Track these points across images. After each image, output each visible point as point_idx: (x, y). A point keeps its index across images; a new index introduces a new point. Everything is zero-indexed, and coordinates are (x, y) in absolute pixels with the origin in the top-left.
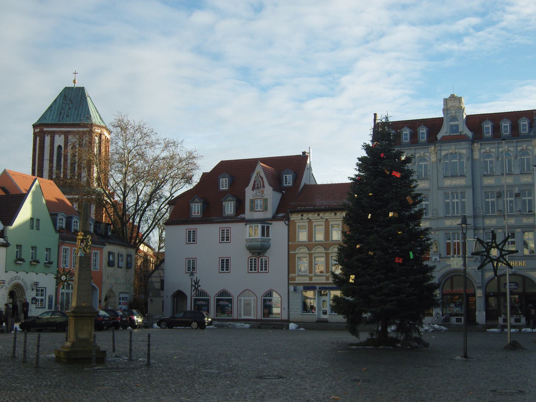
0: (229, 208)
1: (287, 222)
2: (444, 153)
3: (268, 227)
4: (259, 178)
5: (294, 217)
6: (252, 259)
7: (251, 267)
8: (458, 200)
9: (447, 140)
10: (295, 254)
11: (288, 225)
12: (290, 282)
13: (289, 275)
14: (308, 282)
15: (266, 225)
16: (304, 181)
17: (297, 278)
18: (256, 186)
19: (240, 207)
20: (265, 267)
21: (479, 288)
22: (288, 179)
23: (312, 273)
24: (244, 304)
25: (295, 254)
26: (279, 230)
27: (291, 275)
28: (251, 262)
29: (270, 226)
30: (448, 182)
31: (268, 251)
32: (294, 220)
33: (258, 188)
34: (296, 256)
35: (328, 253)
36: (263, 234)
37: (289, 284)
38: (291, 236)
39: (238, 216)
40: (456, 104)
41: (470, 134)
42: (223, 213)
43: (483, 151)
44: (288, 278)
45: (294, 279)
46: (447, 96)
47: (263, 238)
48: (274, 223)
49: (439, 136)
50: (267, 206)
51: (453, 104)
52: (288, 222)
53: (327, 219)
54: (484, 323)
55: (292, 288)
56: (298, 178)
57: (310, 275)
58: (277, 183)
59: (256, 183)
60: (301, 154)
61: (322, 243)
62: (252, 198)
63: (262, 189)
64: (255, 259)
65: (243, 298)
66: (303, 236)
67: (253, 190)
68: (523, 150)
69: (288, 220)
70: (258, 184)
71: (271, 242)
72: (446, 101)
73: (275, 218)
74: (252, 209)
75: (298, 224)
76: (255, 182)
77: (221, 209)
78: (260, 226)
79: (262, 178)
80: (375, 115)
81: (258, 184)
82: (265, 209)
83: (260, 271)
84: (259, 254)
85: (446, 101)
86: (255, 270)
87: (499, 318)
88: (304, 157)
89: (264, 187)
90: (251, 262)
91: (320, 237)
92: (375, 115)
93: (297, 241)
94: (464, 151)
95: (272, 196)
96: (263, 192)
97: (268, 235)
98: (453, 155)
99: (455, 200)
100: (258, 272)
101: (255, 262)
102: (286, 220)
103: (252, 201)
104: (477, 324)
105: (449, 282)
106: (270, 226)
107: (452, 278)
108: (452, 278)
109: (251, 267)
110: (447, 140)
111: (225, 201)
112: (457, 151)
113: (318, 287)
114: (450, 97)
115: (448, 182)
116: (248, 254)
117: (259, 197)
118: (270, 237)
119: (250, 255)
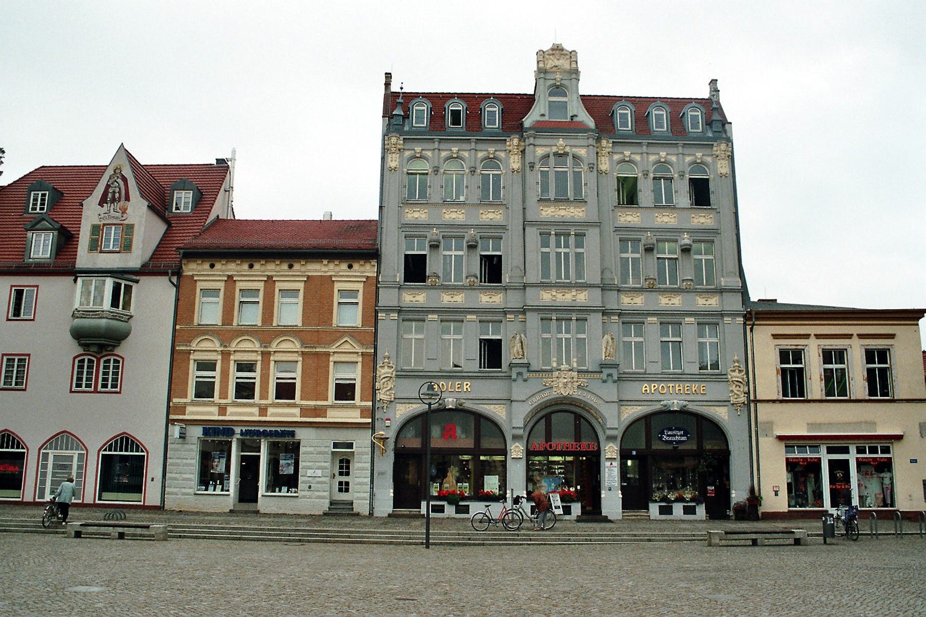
0: (42, 246)
1: (174, 279)
2: (540, 151)
3: (128, 289)
4: (119, 180)
5: (191, 269)
6: (83, 361)
7: (79, 379)
8: (567, 250)
9: (542, 128)
10: (189, 352)
11: (177, 287)
12: (172, 417)
13: (169, 400)
14: (216, 418)
15: (123, 283)
16: (218, 211)
17: (189, 409)
18: (110, 195)
19: (66, 240)
20: (113, 382)
21: (516, 438)
22: (184, 200)
23: (226, 398)
24: (55, 466)
25: (189, 352)
26: (154, 299)
27: (175, 400)
28: (81, 367)
29: (135, 286)
30: (549, 213)
31: (124, 344)
32: (192, 276)
33: (113, 200)
34: (191, 357)
35: (269, 353)
36: (115, 303)
37: (169, 422)
38: (183, 310)
39: (63, 266)
40: (564, 64)
41: (591, 123)
42: (26, 257)
43: (616, 157)
44: (168, 407)
45: (182, 409)
46: (546, 47)
47: (114, 309)
48: (143, 279)
49: (528, 121)
50: (131, 241)
51: (557, 63)
52: (179, 279)
53: (270, 277)
54: (620, 518)
55: (175, 431)
56: (203, 201)
57: (223, 401)
58: (160, 206)
59: (111, 190)
60: (214, 162)
61: (256, 328)
62: (97, 222)
63: (122, 203)
64: (90, 361)
65: (52, 453)
66: (209, 312)
67: (101, 204)
68: (695, 162)
69: (178, 273)
70: (114, 192)
71: (132, 321)
72: (541, 54)
73: (148, 270)
74: (94, 246)
75: (200, 285)
76: (108, 186)
77: (25, 249)
78: (109, 283)
79: (125, 180)
80: (388, 76)
81: (114, 192)
82: (127, 247)
83: (99, 388)
84: (102, 348)
85: (541, 54)
86: (88, 386)
87: (651, 505)
88: (222, 168)
89: (127, 199)
90: (81, 367)
91: (252, 316)
92: (388, 76)
93: (196, 322)
94: (582, 152)
95: (147, 231)
96: (124, 211)
97: (127, 305)
98: (561, 156)
99: (562, 250)
100: (96, 391)
101: (90, 367)
102: (173, 274)
103: (96, 229)
104: (606, 520)
105: (542, 425)
106: (135, 286)
107: (548, 417)
108: (548, 417)
109: (79, 379)
110: (544, 129)
111: (33, 228)
112: (567, 149)
113: (238, 430)
114: (552, 49)
115: (549, 213)
116: (73, 349)
117: (115, 222)
118: (133, 310)
119: (80, 351)
